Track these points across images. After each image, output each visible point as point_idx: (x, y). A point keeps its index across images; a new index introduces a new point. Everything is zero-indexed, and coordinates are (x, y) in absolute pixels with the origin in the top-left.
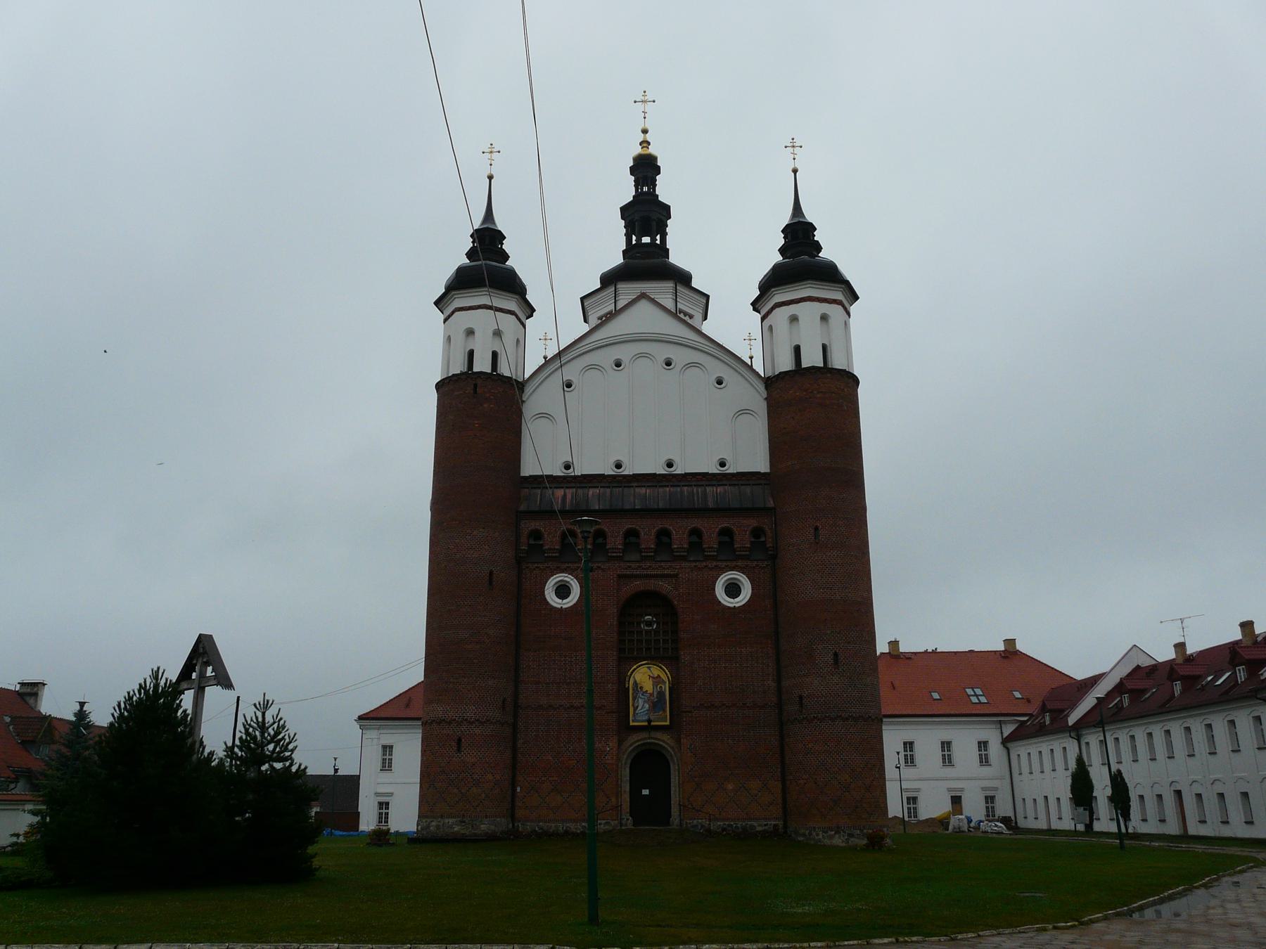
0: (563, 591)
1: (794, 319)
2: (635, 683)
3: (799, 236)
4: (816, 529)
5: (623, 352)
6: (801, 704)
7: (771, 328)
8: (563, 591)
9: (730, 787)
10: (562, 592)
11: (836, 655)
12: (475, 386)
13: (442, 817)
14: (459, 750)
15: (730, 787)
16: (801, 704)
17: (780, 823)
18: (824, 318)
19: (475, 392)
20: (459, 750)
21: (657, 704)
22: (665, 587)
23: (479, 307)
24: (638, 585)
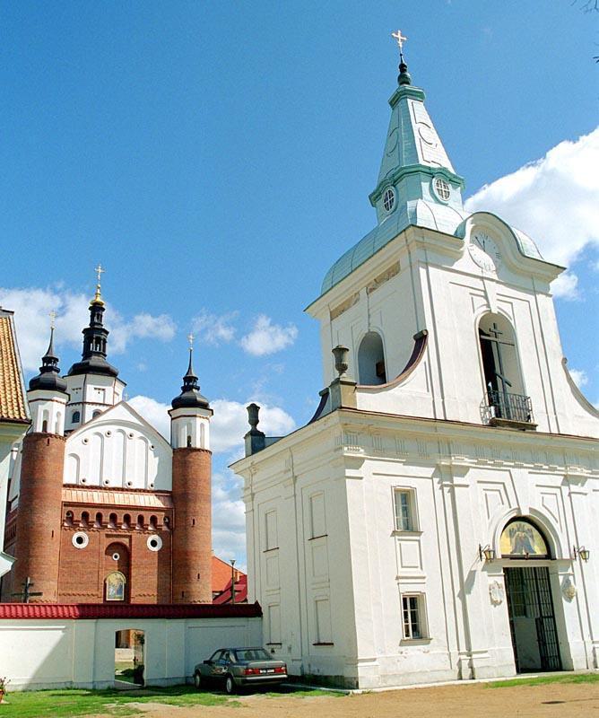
0: (80, 540)
5: (113, 428)
7: (177, 425)
8: (80, 540)
10: (83, 539)
18: (202, 425)
21: (119, 592)
22: (125, 541)
24: (116, 540)
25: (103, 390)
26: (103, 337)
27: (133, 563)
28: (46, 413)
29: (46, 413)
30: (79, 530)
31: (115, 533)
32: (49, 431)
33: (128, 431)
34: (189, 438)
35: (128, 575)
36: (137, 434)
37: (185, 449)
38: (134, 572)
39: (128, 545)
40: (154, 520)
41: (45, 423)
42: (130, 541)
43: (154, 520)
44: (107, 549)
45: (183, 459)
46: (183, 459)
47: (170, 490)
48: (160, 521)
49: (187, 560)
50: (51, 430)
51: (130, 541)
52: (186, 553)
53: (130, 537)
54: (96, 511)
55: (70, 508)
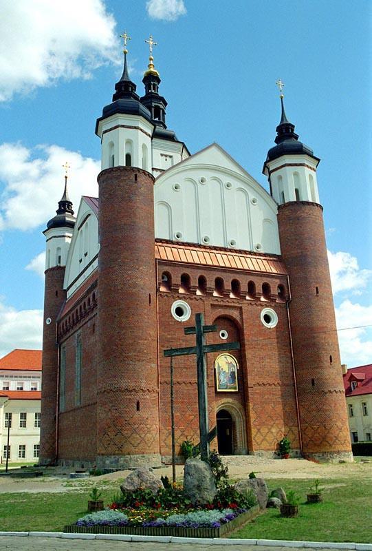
0: (180, 312)
1: (296, 174)
2: (219, 367)
3: (285, 131)
4: (317, 288)
5: (208, 175)
6: (313, 384)
7: (280, 178)
8: (180, 312)
9: (274, 430)
10: (184, 309)
11: (331, 357)
12: (136, 175)
13: (129, 454)
14: (138, 409)
15: (274, 430)
16: (313, 384)
17: (299, 451)
19: (136, 179)
20: (138, 409)
22: (235, 314)
23: (135, 128)
24: (223, 312)
25: (171, 157)
26: (161, 106)
27: (246, 342)
28: (129, 142)
29: (129, 142)
30: (180, 299)
31: (222, 303)
32: (134, 165)
33: (226, 179)
34: (297, 191)
35: (241, 358)
36: (236, 184)
37: (291, 204)
38: (249, 354)
39: (238, 319)
40: (266, 288)
41: (128, 157)
42: (241, 314)
43: (266, 288)
44: (216, 319)
45: (294, 218)
46: (294, 218)
47: (279, 253)
48: (275, 291)
49: (314, 337)
50: (137, 163)
51: (241, 314)
52: (312, 330)
53: (241, 308)
54: (199, 273)
55: (166, 268)
